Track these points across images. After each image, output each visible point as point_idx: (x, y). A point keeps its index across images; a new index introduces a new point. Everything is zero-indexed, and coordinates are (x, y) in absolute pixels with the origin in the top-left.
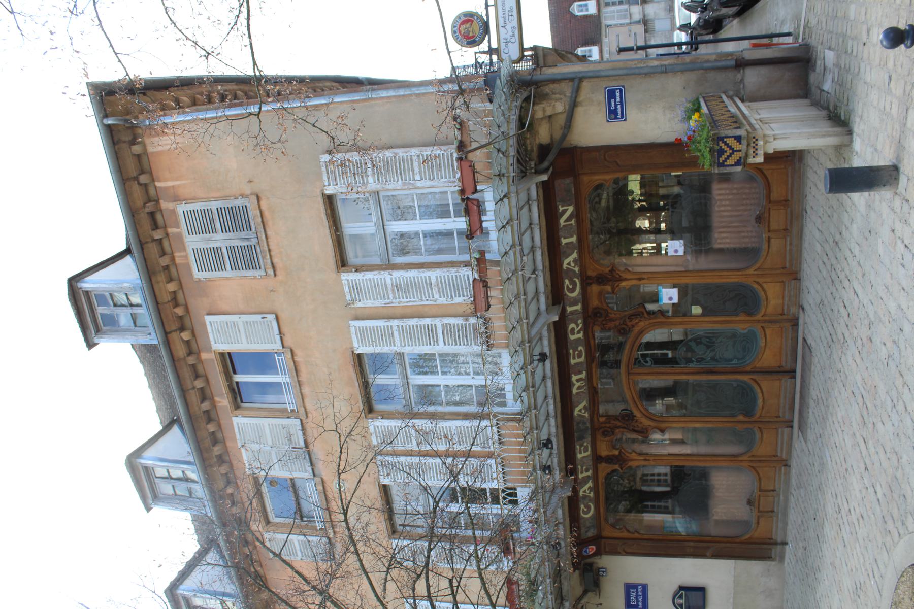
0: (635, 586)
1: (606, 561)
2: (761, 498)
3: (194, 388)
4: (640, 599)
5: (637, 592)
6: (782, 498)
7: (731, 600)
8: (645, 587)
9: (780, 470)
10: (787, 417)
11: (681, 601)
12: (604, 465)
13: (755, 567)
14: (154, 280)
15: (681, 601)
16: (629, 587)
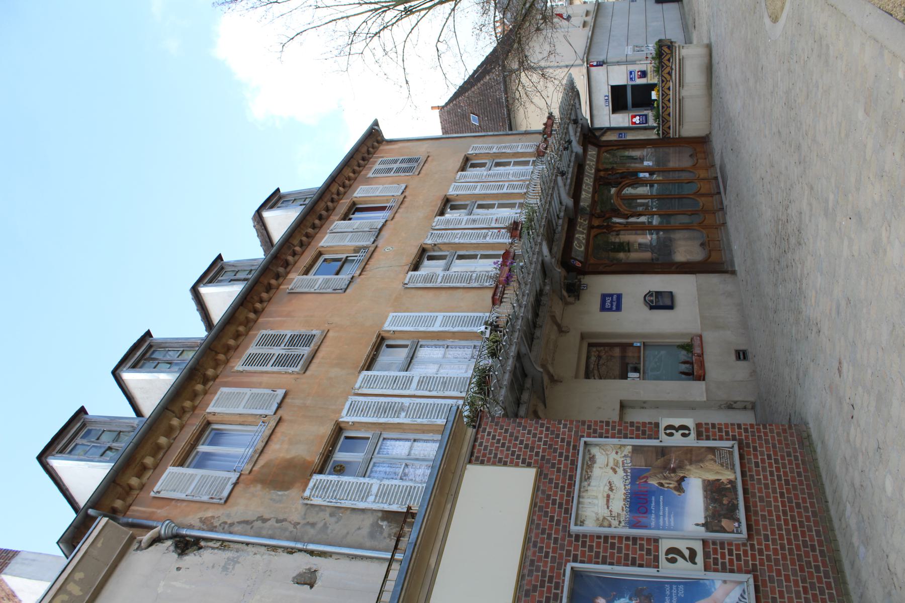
0: (611, 295)
1: (588, 280)
2: (710, 242)
3: (326, 203)
4: (615, 304)
5: (612, 299)
6: (725, 239)
7: (697, 302)
8: (619, 297)
9: (721, 229)
10: (719, 207)
11: (652, 298)
12: (595, 230)
13: (713, 280)
14: (346, 167)
15: (652, 298)
16: (604, 297)
